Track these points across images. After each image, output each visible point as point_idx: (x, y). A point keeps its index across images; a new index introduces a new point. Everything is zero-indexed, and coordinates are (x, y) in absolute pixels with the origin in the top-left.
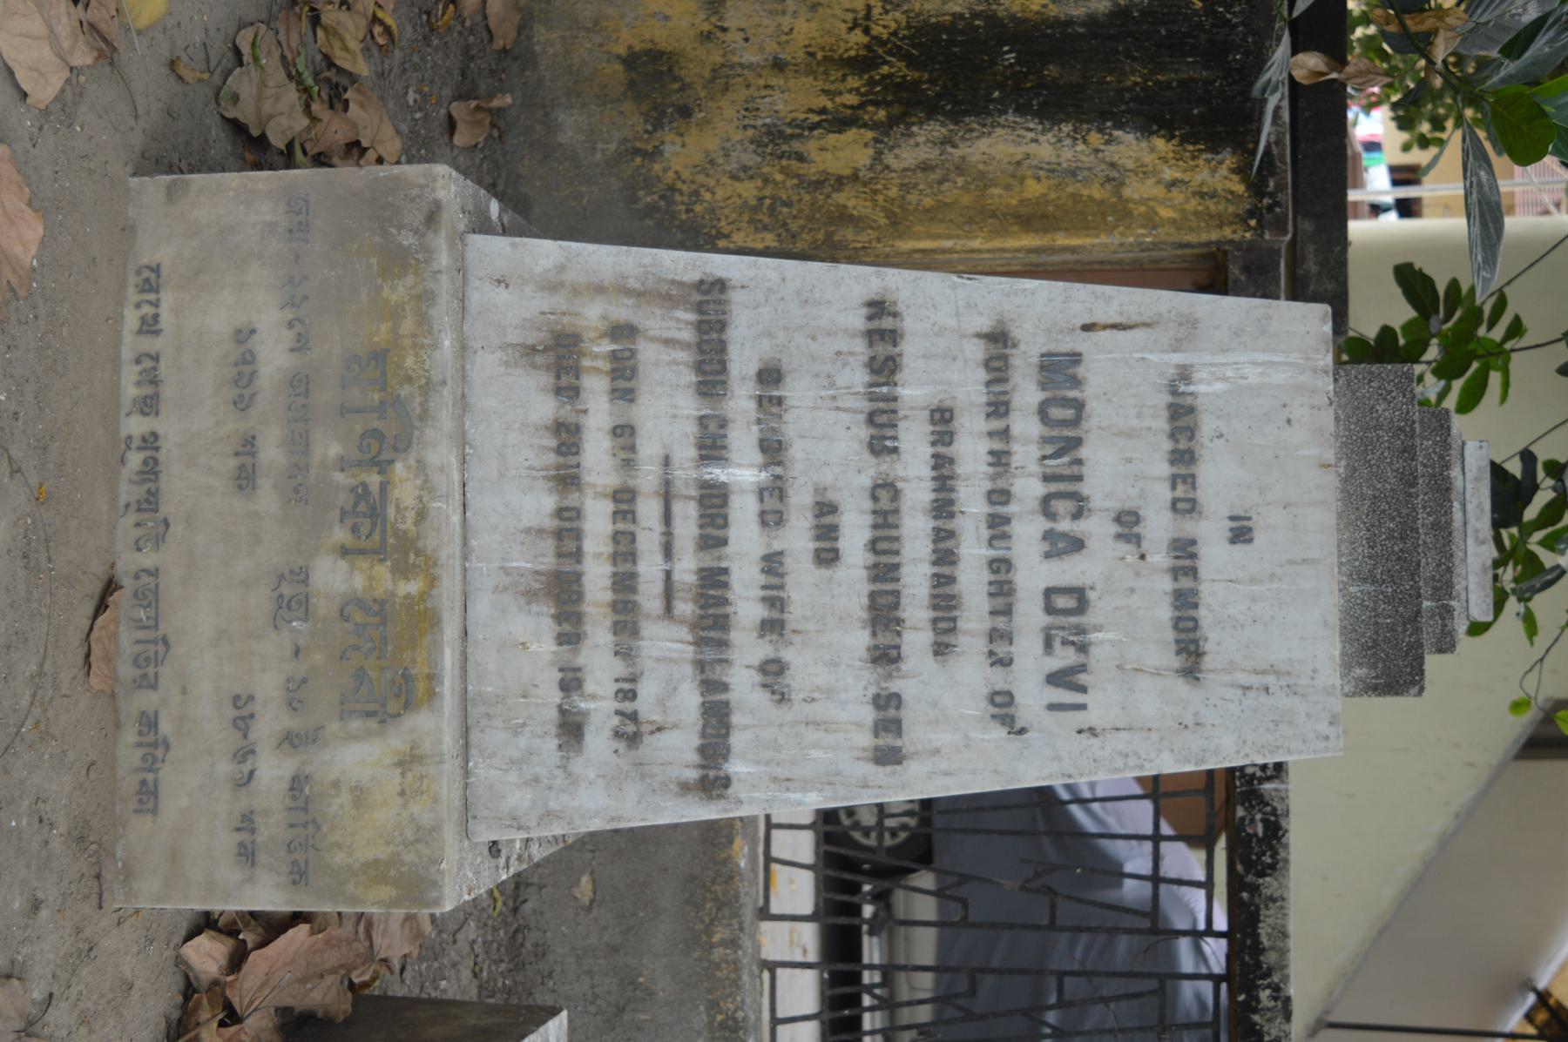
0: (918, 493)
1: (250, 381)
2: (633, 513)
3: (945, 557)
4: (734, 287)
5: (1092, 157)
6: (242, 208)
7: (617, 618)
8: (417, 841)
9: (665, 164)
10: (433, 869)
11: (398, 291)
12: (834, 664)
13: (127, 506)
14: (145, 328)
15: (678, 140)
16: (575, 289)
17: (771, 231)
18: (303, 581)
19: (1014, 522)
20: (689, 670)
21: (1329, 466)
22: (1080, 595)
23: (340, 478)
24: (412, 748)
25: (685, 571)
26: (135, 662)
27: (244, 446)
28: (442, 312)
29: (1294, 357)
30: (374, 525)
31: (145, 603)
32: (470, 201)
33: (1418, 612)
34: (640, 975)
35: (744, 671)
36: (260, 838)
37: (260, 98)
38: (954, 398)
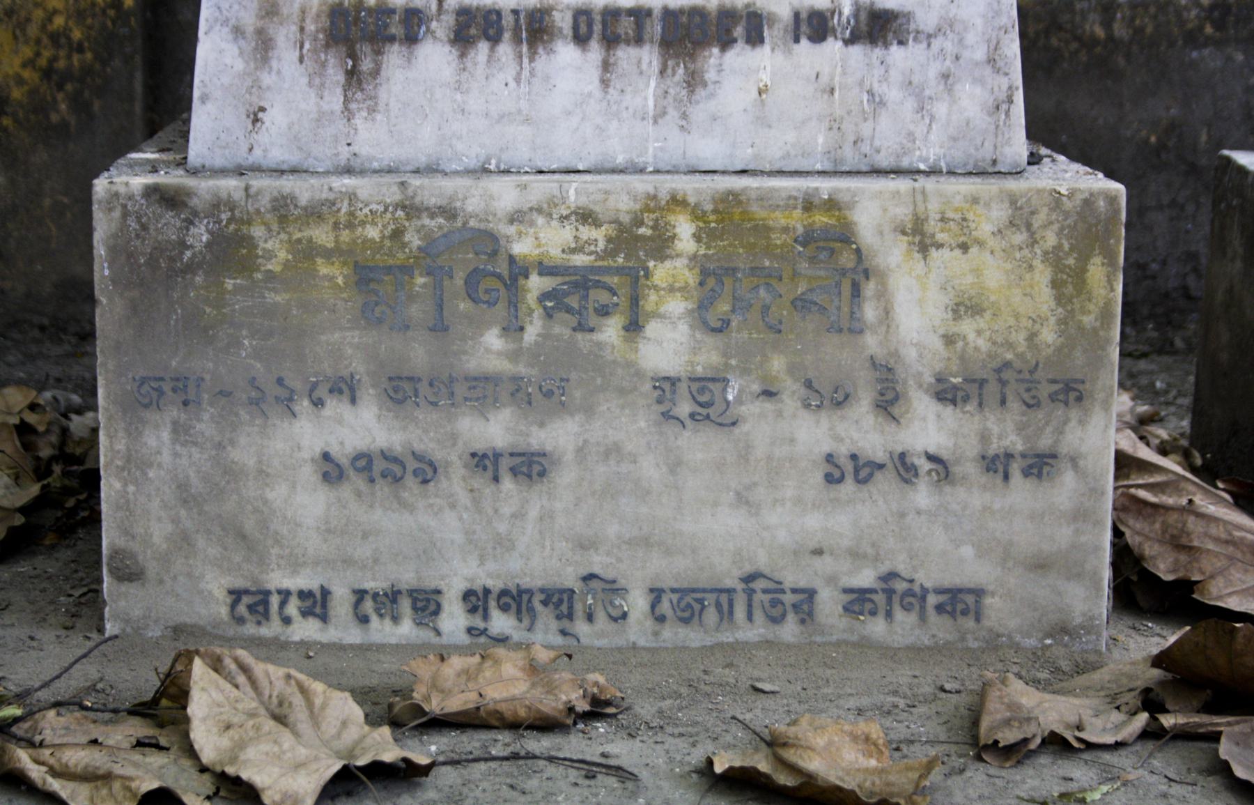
1: (396, 460)
6: (151, 474)
8: (1029, 226)
9: (12, 83)
10: (1068, 204)
13: (564, 633)
14: (318, 610)
16: (267, 14)
18: (673, 384)
23: (532, 332)
24: (904, 233)
26: (777, 620)
27: (485, 468)
28: (304, 190)
30: (598, 285)
31: (697, 607)
34: (1146, 141)
36: (1019, 446)
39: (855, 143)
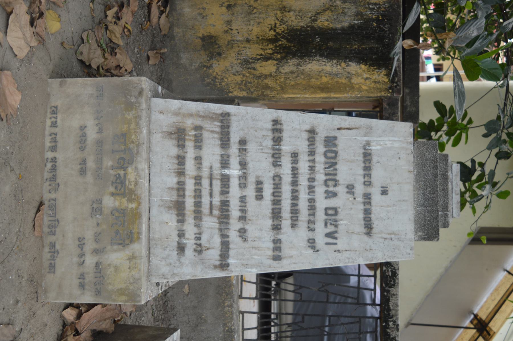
0: (287, 179)
1: (85, 142)
2: (201, 183)
3: (295, 198)
5: (342, 70)
6: (82, 89)
7: (195, 215)
8: (134, 282)
11: (130, 116)
12: (261, 230)
13: (47, 179)
14: (53, 125)
15: (217, 63)
17: (245, 91)
19: (316, 188)
20: (217, 231)
21: (411, 172)
22: (335, 209)
23: (112, 172)
24: (133, 254)
26: (49, 227)
27: (83, 162)
28: (143, 122)
29: (401, 139)
30: (122, 186)
31: (52, 209)
32: (153, 87)
33: (438, 216)
36: (86, 281)
37: (89, 53)
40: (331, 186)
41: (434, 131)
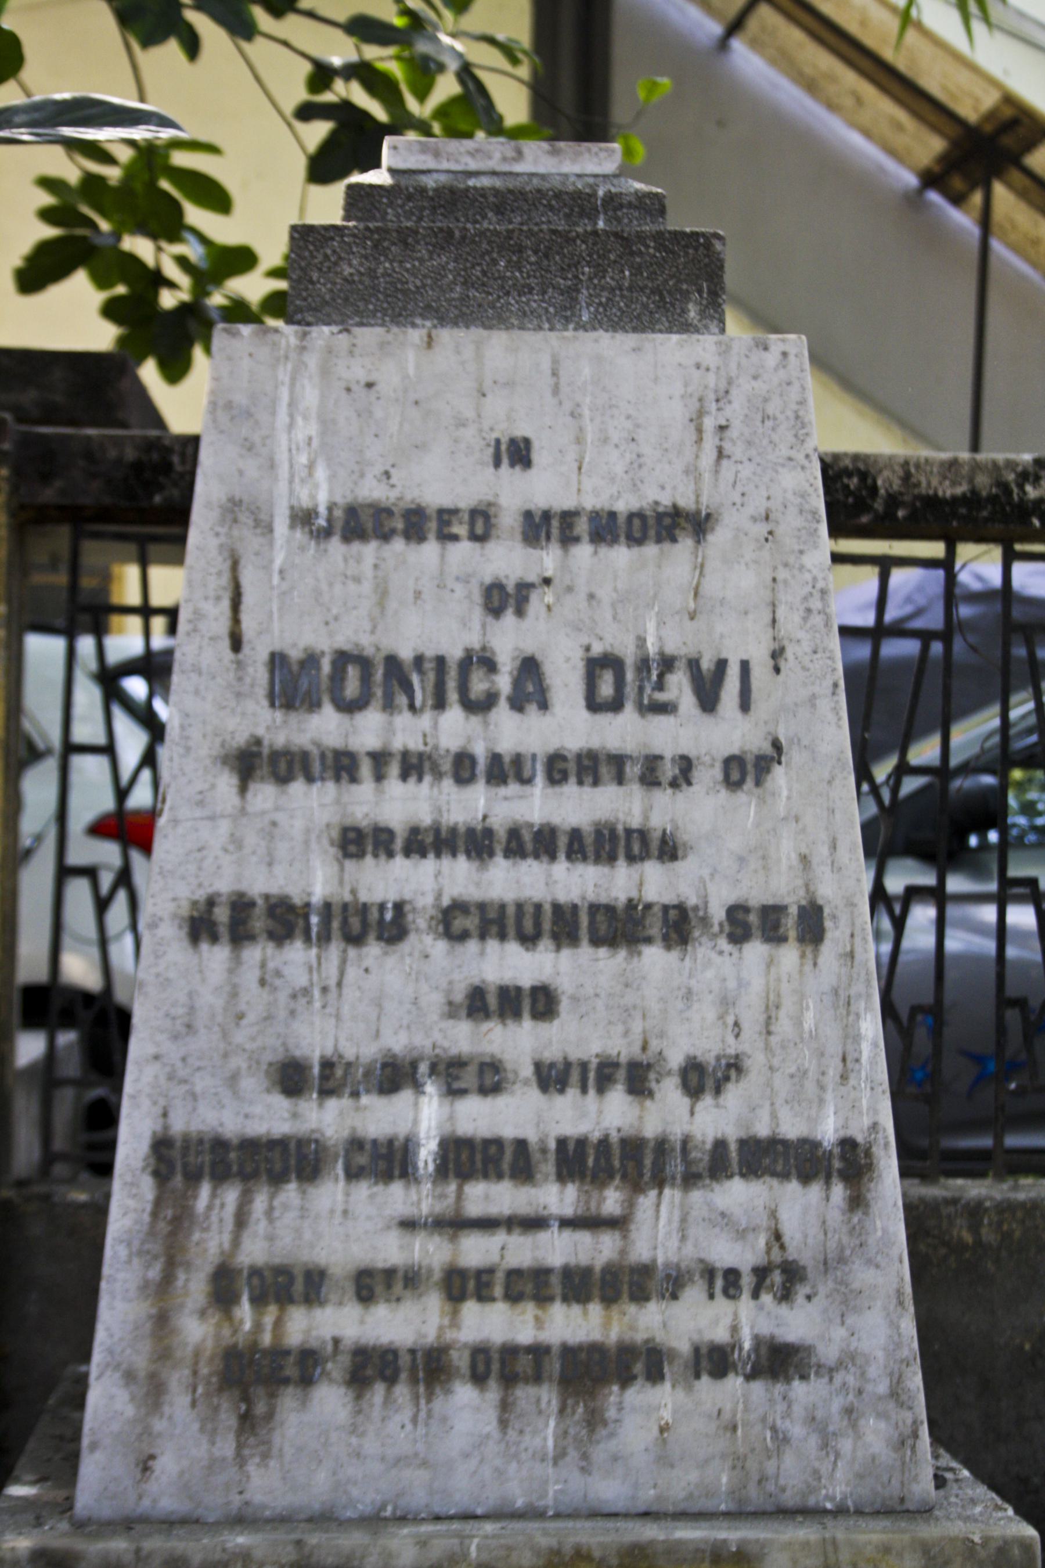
4: (166, 1128)
7: (625, 1296)
10: (982, 1554)
12: (689, 995)
19: (499, 749)
20: (696, 1196)
21: (430, 336)
25: (561, 1200)
29: (283, 374)
33: (616, 235)
34: (1021, 1348)
35: (698, 1117)
38: (328, 826)
39: (760, 1482)
40: (493, 682)
41: (156, 295)
